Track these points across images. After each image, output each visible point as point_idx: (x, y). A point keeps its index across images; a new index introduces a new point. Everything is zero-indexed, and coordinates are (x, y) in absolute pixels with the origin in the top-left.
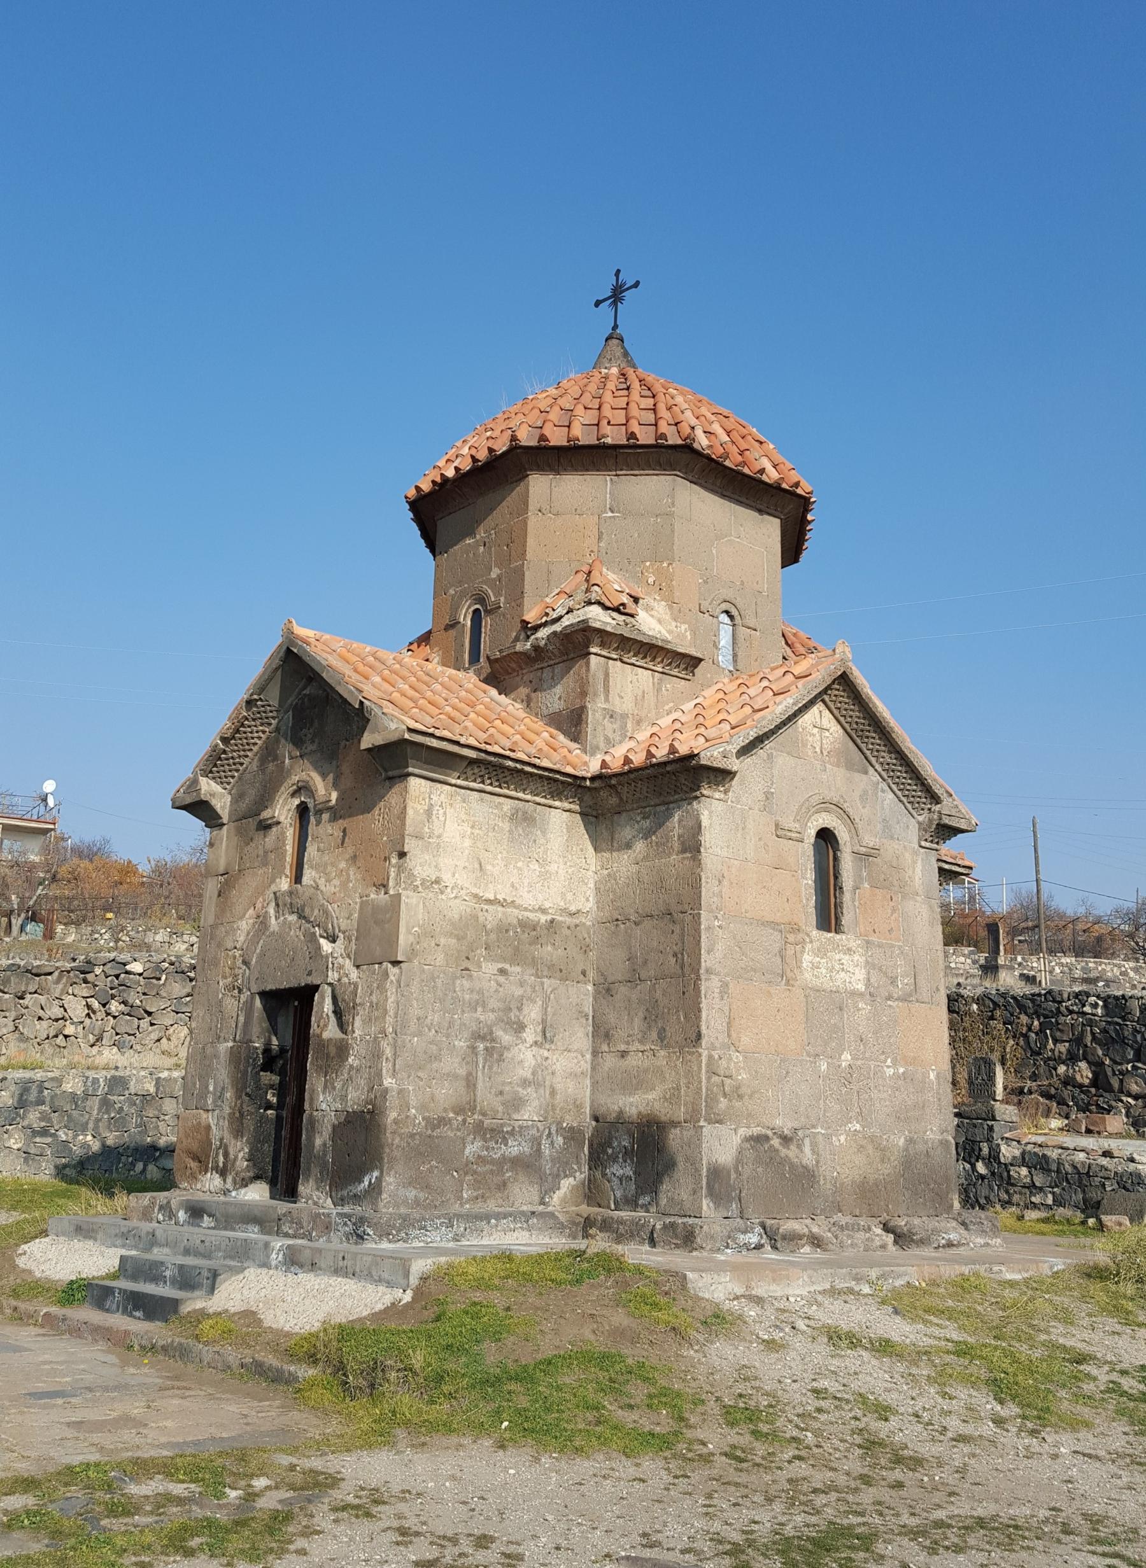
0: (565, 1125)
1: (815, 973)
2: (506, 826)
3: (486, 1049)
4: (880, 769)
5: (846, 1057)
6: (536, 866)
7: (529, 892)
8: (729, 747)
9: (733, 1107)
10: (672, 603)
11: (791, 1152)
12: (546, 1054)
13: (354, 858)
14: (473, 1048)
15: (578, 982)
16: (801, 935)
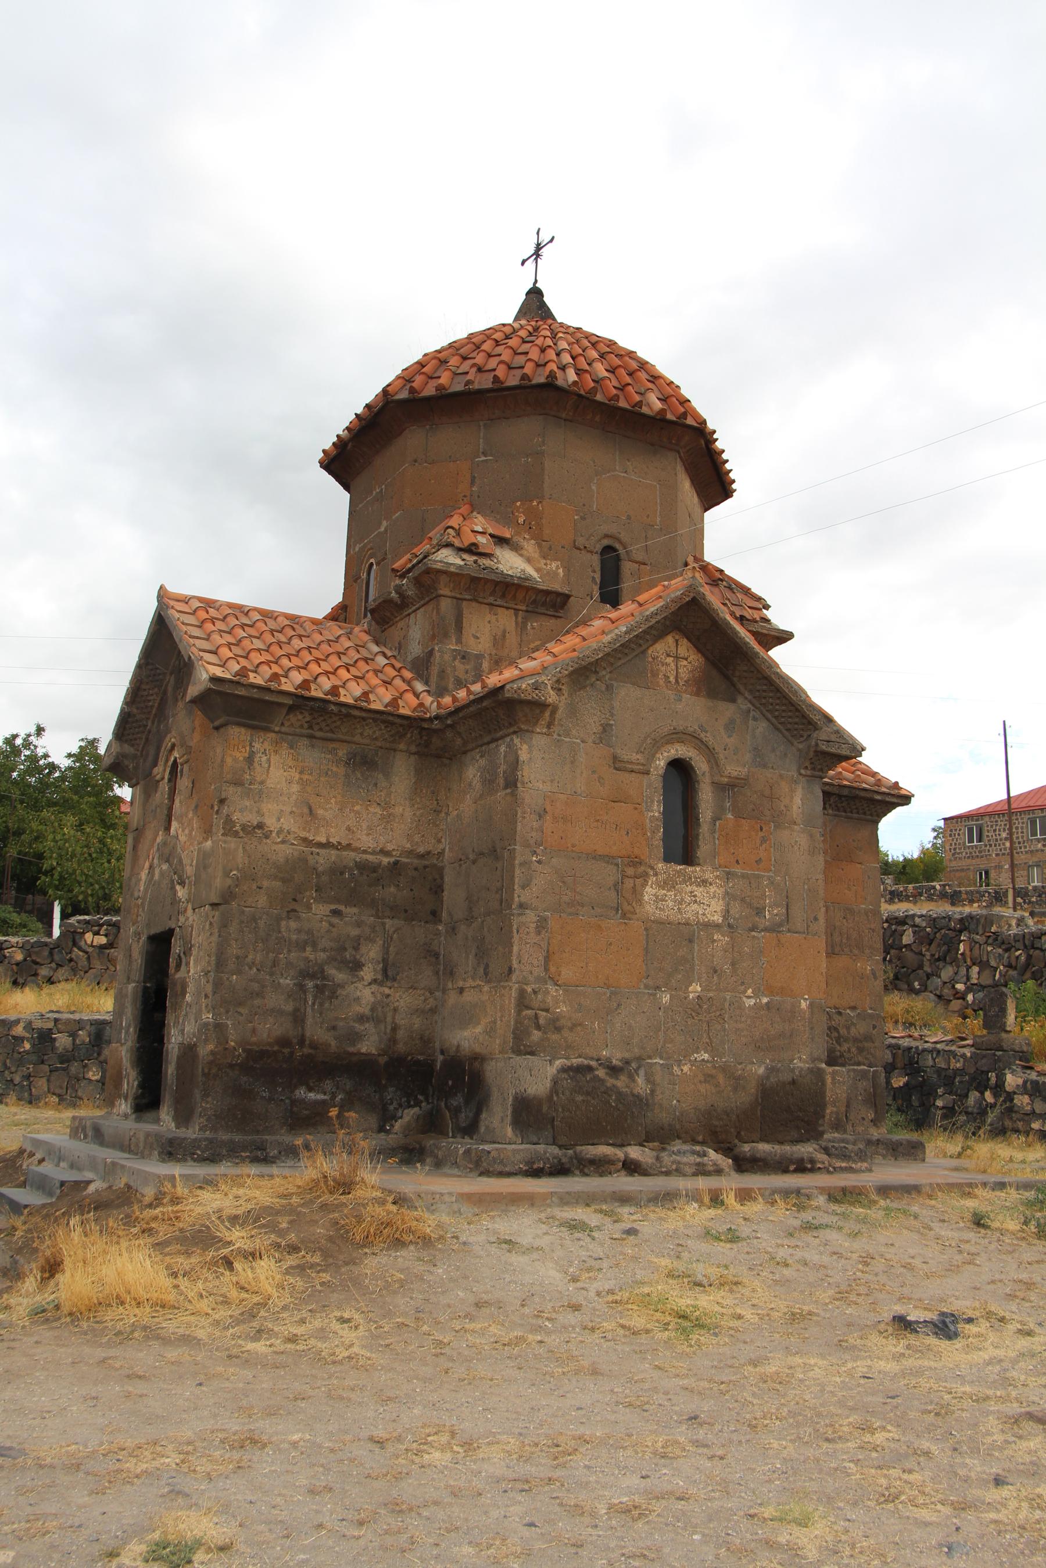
0: (410, 1058)
1: (660, 905)
2: (341, 770)
3: (316, 986)
4: (750, 697)
5: (695, 989)
6: (378, 810)
7: (368, 835)
8: (543, 678)
9: (548, 1039)
10: (539, 539)
11: (621, 1083)
12: (387, 991)
13: (197, 807)
14: (301, 987)
15: (426, 922)
16: (643, 868)
